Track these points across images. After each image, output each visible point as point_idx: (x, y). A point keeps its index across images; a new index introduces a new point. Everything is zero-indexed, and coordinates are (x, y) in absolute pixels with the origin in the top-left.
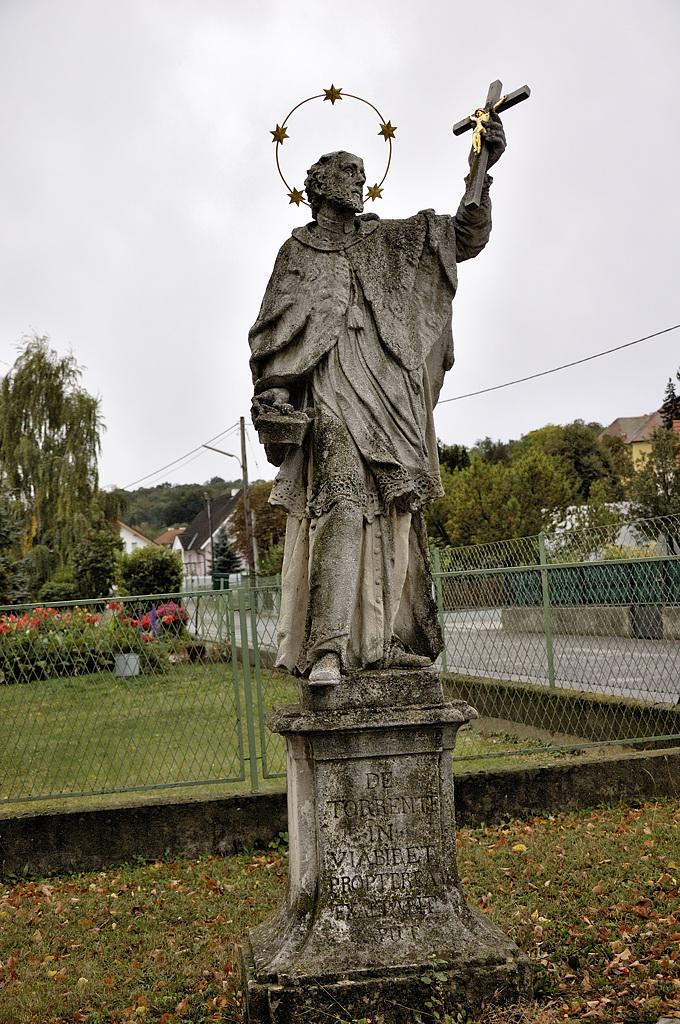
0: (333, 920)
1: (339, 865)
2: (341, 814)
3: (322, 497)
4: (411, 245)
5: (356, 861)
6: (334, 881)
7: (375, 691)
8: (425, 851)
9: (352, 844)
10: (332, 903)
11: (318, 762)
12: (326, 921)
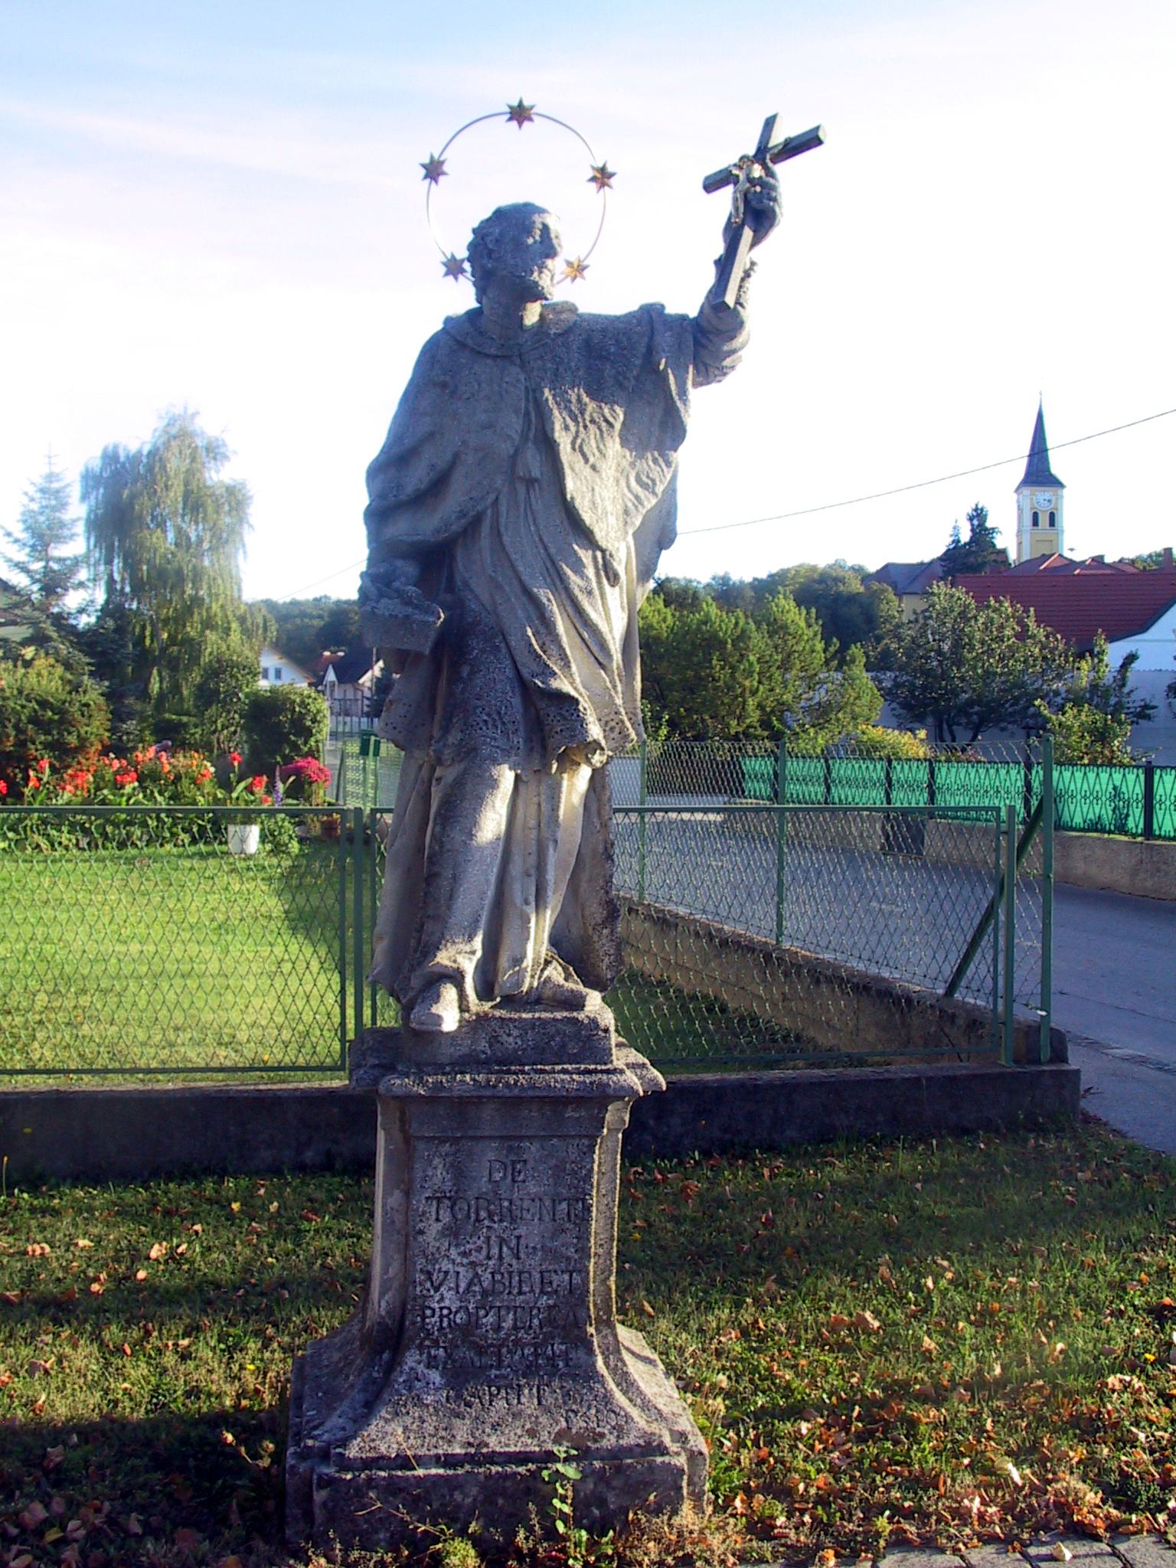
0: (421, 1368)
1: (437, 1289)
2: (446, 1217)
3: (454, 737)
4: (624, 356)
5: (463, 1286)
6: (428, 1312)
7: (511, 1039)
8: (566, 1277)
9: (459, 1260)
11: (419, 1138)
12: (412, 1369)
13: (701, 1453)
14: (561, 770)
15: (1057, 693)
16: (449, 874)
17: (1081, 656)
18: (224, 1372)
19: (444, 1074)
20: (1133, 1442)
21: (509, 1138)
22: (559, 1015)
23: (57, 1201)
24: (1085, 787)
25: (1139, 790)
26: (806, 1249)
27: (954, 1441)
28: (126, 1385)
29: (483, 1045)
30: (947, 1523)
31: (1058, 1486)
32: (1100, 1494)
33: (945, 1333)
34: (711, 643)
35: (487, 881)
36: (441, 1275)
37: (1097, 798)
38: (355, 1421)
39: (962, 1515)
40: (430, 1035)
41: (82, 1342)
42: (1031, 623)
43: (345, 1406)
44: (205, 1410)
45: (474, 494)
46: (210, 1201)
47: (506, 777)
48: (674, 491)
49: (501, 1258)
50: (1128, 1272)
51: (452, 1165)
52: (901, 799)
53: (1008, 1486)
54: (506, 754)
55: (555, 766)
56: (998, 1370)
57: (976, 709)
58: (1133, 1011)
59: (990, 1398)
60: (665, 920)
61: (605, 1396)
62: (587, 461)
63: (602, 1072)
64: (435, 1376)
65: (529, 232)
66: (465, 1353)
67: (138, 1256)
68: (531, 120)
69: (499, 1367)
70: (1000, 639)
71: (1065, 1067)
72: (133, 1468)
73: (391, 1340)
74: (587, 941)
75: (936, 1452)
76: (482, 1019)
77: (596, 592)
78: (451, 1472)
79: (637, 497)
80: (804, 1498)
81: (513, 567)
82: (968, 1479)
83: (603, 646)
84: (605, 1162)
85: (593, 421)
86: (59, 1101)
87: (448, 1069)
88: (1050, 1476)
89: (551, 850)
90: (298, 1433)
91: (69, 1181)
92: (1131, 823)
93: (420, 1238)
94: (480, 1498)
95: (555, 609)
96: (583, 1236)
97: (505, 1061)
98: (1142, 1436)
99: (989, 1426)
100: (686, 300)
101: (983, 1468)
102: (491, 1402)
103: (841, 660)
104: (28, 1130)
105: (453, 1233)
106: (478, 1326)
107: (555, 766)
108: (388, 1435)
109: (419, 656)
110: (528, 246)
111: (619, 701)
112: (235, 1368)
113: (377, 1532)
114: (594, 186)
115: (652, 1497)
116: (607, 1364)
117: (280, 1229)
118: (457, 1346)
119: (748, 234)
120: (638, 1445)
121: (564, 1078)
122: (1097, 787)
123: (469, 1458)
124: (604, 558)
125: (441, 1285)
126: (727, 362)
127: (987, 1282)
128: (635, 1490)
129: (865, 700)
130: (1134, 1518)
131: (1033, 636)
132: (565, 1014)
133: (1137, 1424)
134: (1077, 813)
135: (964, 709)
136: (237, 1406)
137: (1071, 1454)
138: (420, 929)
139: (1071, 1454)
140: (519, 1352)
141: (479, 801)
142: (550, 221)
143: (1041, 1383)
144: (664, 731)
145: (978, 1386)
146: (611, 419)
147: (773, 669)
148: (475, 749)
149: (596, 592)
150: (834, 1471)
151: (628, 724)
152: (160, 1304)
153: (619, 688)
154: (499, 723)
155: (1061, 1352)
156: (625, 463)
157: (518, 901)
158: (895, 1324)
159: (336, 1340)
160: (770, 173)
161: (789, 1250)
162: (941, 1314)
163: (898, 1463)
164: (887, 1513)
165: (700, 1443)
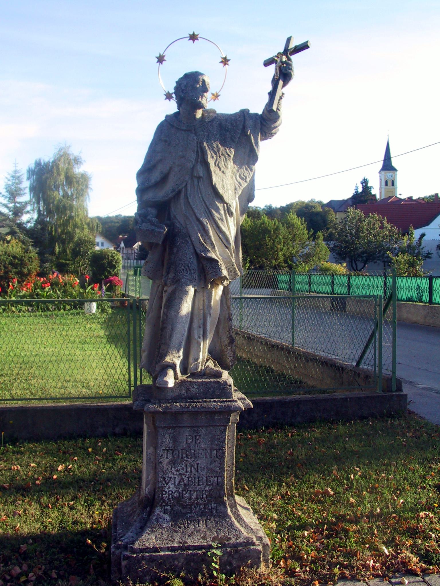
0: (161, 514)
1: (167, 484)
2: (170, 457)
3: (171, 275)
5: (177, 482)
6: (164, 493)
7: (194, 390)
8: (216, 479)
9: (175, 473)
10: (161, 505)
11: (159, 427)
12: (158, 514)
13: (267, 545)
14: (212, 287)
15: (395, 249)
16: (170, 327)
17: (404, 235)
18: (87, 514)
19: (169, 403)
20: (430, 538)
21: (194, 427)
22: (212, 380)
23: (22, 449)
24: (407, 285)
25: (427, 286)
26: (305, 464)
27: (363, 538)
28: (50, 520)
29: (183, 392)
30: (361, 570)
31: (402, 555)
32: (418, 558)
33: (358, 496)
34: (266, 231)
35: (185, 330)
36: (169, 479)
37: (411, 289)
38: (137, 534)
39: (366, 567)
40: (164, 388)
41: (33, 503)
42: (385, 222)
43: (133, 528)
44: (80, 529)
45: (177, 183)
46: (80, 448)
47: (191, 290)
48: (254, 180)
49: (191, 472)
50: (427, 472)
51: (172, 437)
52: (337, 290)
53: (383, 555)
54: (191, 282)
55: (210, 286)
56: (379, 510)
57: (365, 255)
58: (426, 370)
59: (376, 521)
60: (249, 338)
61: (231, 523)
62: (220, 170)
63: (229, 401)
64: (167, 517)
65: (198, 83)
66: (178, 508)
67: (53, 470)
68: (198, 40)
69: (191, 513)
70: (374, 229)
71: (402, 393)
72: (53, 552)
73: (150, 503)
74: (222, 351)
75: (356, 542)
76: (183, 382)
77: (225, 220)
78: (173, 553)
79: (240, 183)
80: (306, 560)
81: (193, 211)
82: (368, 553)
83: (227, 240)
84: (230, 435)
85: (222, 154)
86: (23, 411)
87: (170, 401)
88: (399, 551)
89: (208, 317)
90: (115, 539)
91: (27, 441)
92: (424, 298)
93: (161, 465)
94: (185, 563)
95: (209, 226)
96: (222, 463)
97: (192, 398)
98: (433, 536)
99: (376, 532)
100: (257, 108)
101: (374, 549)
102: (188, 526)
103: (314, 237)
104: (11, 422)
105: (173, 463)
106: (183, 498)
107: (210, 286)
108: (150, 539)
109: (157, 244)
110: (197, 88)
111: (233, 261)
112: (91, 513)
113: (146, 576)
114: (222, 64)
115: (249, 562)
116: (231, 511)
117: (107, 459)
118: (175, 505)
119: (281, 83)
120: (244, 542)
121: (215, 404)
122: (411, 285)
123: (180, 548)
124: (227, 206)
125: (168, 483)
126: (273, 131)
127: (374, 476)
128: (243, 558)
129: (323, 252)
130: (431, 567)
131: (386, 228)
132: (214, 380)
133: (431, 531)
134: (403, 294)
135: (360, 255)
136: (92, 527)
137: (407, 543)
138: (159, 349)
139: (407, 543)
140: (198, 507)
141: (181, 300)
142: (206, 78)
143: (395, 515)
144: (248, 265)
145: (371, 516)
146: (229, 154)
147: (289, 241)
148: (179, 280)
149: (225, 220)
150: (318, 550)
151: (237, 269)
152: (62, 488)
153: (234, 256)
154: (188, 270)
155: (402, 503)
156: (235, 170)
157: (196, 337)
158: (339, 493)
159: (129, 502)
160: (289, 59)
161: (299, 464)
162: (356, 489)
163: (341, 547)
164: (338, 566)
165: (267, 541)
